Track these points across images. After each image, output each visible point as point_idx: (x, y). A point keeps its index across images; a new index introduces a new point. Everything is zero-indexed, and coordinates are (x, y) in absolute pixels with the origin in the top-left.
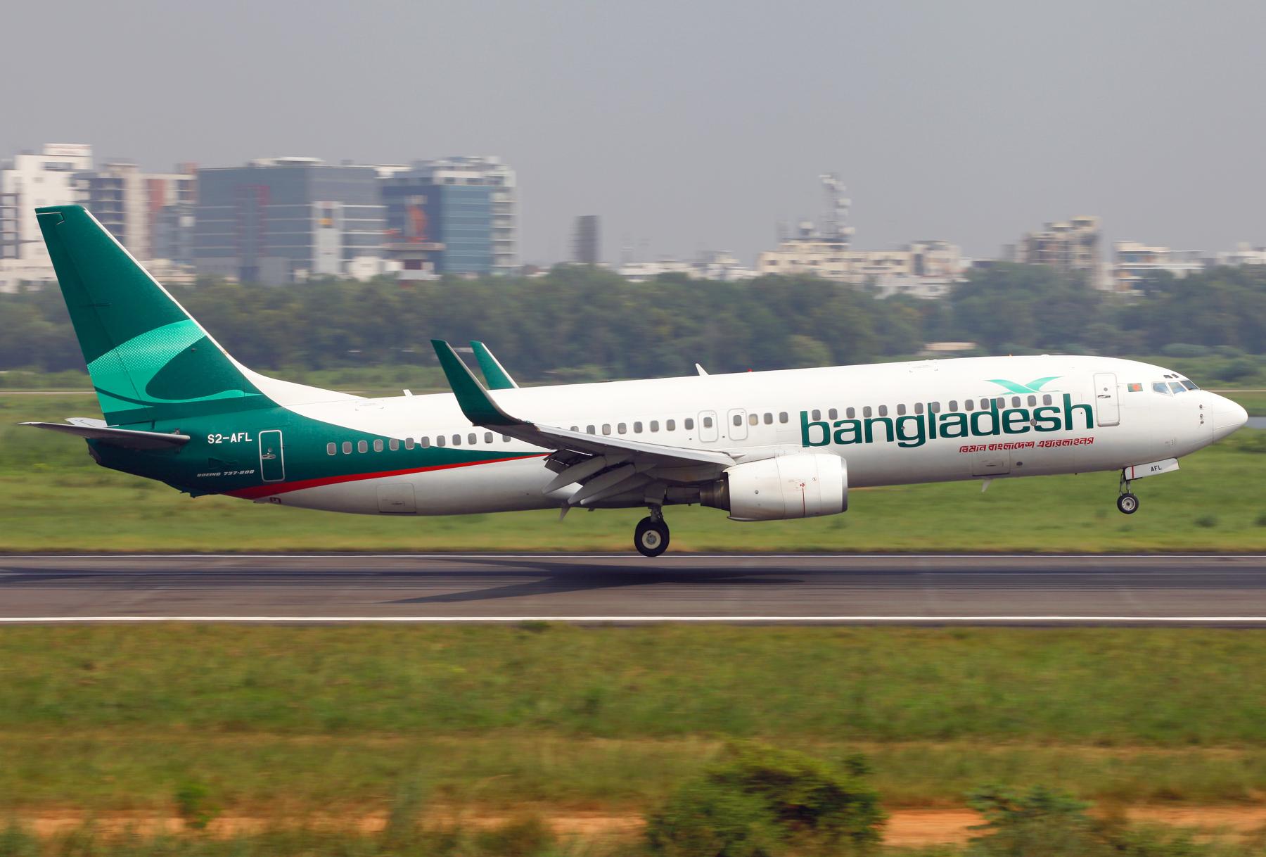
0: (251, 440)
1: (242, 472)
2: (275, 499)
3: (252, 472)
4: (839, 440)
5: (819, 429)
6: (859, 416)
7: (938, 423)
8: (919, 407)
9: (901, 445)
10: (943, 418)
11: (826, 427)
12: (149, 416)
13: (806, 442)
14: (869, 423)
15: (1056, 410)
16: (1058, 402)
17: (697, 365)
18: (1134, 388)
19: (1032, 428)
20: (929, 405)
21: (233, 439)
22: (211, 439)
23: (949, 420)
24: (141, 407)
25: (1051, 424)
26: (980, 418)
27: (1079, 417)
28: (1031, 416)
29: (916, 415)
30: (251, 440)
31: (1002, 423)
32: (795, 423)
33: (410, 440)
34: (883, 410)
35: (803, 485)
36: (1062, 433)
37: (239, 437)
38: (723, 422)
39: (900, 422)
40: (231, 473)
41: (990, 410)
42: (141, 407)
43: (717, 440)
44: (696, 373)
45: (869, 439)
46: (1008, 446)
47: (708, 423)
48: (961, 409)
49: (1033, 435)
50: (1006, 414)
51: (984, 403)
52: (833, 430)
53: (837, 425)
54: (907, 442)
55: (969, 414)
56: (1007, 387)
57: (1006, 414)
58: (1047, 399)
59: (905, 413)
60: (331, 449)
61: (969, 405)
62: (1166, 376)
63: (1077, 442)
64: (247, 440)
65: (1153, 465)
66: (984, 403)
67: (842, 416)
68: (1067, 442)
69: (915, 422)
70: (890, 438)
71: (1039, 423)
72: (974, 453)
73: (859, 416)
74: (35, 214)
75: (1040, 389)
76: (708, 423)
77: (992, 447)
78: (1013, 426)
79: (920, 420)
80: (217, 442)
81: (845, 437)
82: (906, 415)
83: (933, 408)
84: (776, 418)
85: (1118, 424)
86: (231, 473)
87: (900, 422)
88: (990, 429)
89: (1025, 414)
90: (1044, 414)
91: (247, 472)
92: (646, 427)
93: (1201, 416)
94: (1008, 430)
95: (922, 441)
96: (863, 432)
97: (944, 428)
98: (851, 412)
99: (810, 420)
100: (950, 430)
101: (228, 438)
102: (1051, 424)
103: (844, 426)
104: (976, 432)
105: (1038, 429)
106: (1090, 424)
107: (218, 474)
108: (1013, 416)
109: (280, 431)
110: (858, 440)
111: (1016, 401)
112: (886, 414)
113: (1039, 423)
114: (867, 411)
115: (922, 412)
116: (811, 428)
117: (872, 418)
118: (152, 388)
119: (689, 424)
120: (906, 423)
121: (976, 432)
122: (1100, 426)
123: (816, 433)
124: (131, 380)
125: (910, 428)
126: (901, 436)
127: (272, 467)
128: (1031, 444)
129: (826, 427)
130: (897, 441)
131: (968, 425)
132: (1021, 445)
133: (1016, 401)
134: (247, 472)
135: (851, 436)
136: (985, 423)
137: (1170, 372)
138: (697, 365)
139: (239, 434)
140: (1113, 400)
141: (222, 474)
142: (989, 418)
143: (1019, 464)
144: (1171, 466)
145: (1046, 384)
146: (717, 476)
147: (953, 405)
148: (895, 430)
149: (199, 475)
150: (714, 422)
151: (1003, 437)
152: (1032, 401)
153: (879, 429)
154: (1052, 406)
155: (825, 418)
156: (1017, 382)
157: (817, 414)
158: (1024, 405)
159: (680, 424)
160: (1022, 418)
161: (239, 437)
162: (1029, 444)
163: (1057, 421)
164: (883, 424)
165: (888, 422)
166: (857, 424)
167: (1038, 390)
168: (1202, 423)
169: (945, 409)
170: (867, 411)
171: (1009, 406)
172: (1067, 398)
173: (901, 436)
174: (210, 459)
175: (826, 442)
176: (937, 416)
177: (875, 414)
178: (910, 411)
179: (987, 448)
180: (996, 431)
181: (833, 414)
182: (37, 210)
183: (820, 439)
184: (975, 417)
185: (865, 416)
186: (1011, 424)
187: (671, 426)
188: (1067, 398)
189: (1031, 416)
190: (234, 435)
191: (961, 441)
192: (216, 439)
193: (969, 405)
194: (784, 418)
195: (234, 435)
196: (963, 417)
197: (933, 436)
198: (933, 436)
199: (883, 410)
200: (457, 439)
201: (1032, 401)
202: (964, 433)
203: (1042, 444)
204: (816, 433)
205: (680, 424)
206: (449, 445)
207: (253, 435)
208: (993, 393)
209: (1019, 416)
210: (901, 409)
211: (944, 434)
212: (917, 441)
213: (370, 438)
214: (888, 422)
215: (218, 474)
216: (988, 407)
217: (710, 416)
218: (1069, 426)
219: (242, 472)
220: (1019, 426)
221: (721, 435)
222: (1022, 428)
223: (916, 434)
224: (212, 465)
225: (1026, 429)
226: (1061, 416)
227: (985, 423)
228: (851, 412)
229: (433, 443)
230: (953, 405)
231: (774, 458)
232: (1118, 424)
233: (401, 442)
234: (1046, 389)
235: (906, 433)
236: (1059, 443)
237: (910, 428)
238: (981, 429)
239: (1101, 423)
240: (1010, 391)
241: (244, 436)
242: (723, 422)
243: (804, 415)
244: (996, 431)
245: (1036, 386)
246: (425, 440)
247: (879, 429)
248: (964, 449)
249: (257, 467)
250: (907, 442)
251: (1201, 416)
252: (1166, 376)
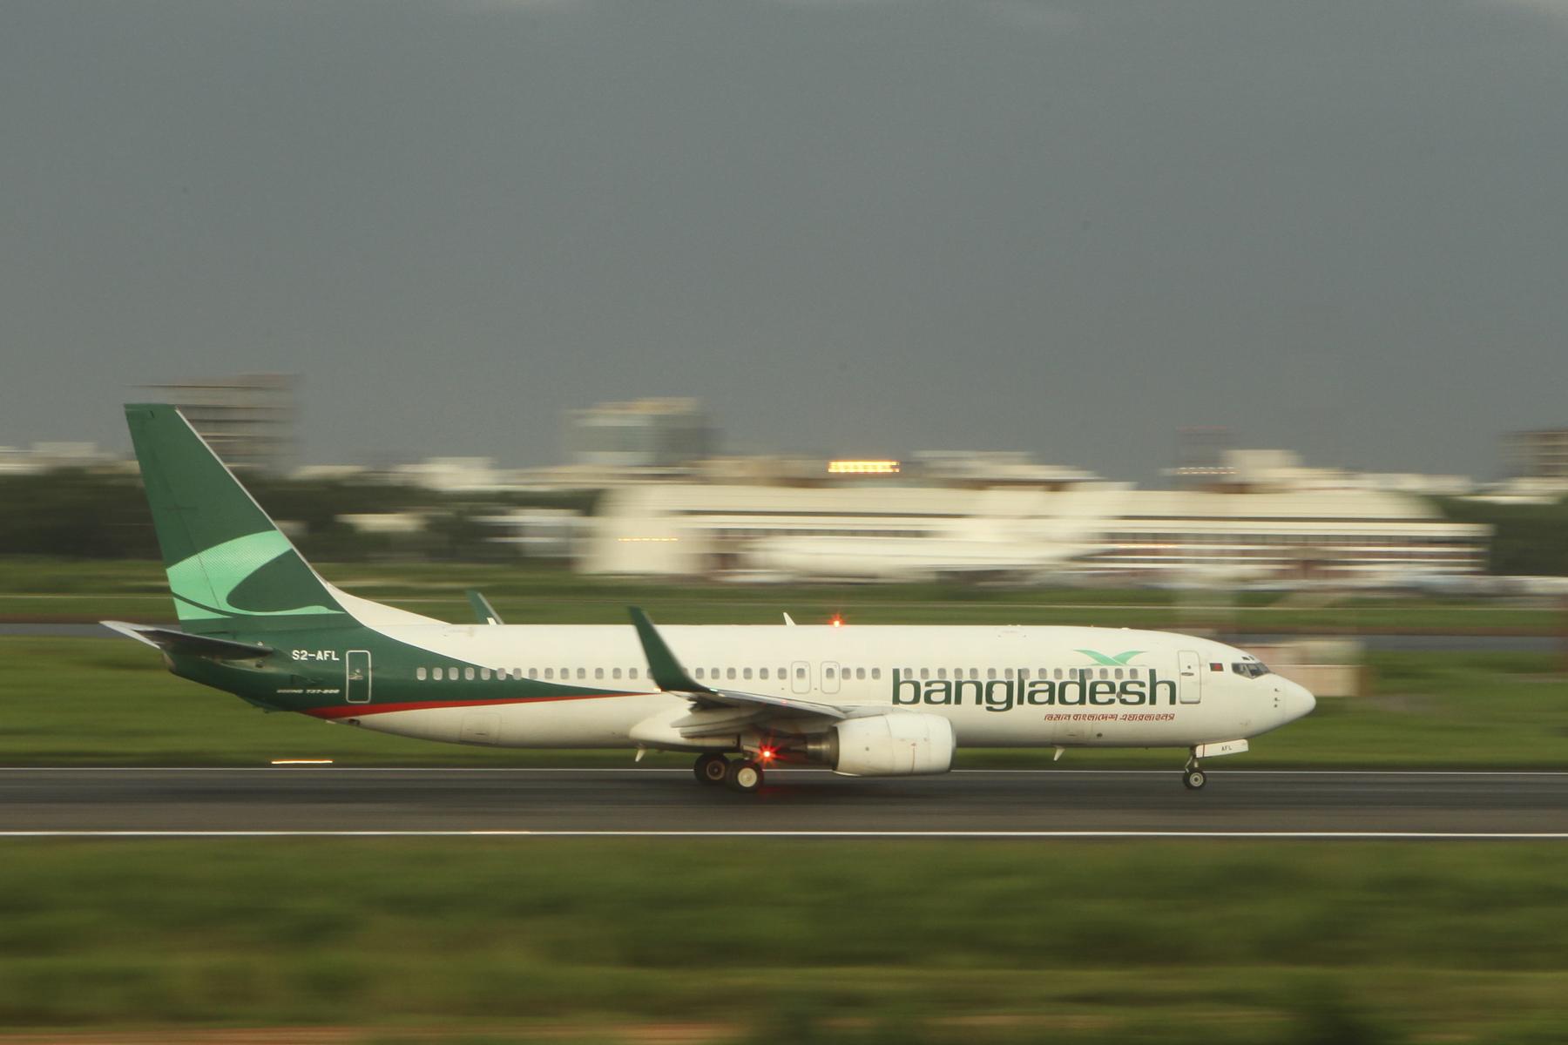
0: (338, 659)
1: (326, 691)
2: (352, 721)
3: (337, 691)
4: (928, 700)
5: (911, 688)
6: (952, 678)
7: (1027, 690)
8: (1009, 672)
9: (989, 709)
10: (1032, 684)
11: (917, 686)
12: (228, 625)
13: (896, 700)
14: (959, 685)
15: (1142, 684)
16: (1145, 678)
17: (786, 615)
18: (1216, 667)
19: (1117, 701)
20: (1020, 671)
21: (319, 656)
22: (296, 655)
23: (1038, 687)
24: (220, 616)
25: (1136, 698)
26: (1068, 687)
27: (1163, 692)
28: (1118, 689)
29: (1006, 681)
30: (338, 659)
31: (1088, 694)
32: (887, 680)
33: (502, 670)
34: (974, 671)
35: (914, 745)
36: (1146, 708)
37: (326, 655)
38: (816, 674)
39: (990, 686)
40: (314, 691)
41: (1078, 680)
42: (220, 616)
43: (808, 693)
44: (783, 622)
45: (958, 701)
46: (1092, 717)
47: (801, 672)
48: (1050, 677)
49: (1117, 708)
50: (1094, 685)
51: (1072, 671)
52: (924, 689)
53: (928, 684)
54: (995, 707)
56: (1097, 659)
57: (1094, 685)
58: (1134, 672)
59: (994, 678)
60: (421, 675)
61: (1058, 672)
62: (1245, 658)
63: (1159, 717)
64: (334, 659)
65: (1224, 744)
66: (1072, 671)
67: (934, 676)
68: (1149, 717)
69: (1005, 687)
70: (979, 701)
71: (1124, 696)
72: (1058, 722)
73: (952, 678)
74: (123, 410)
75: (1128, 662)
76: (801, 672)
77: (1076, 717)
78: (1099, 698)
79: (1010, 685)
80: (302, 658)
81: (934, 697)
82: (997, 679)
84: (868, 673)
85: (1198, 702)
86: (314, 691)
87: (990, 686)
88: (1077, 699)
89: (1112, 686)
90: (1130, 688)
91: (331, 691)
92: (740, 673)
93: (1276, 699)
94: (1093, 701)
95: (1009, 706)
96: (953, 694)
97: (1032, 695)
98: (942, 672)
99: (902, 678)
100: (1038, 697)
101: (310, 655)
102: (1136, 698)
103: (934, 686)
104: (1063, 701)
105: (1123, 702)
106: (1173, 701)
107: (300, 691)
108: (1100, 688)
109: (369, 653)
110: (947, 701)
111: (1104, 672)
112: (945, 677)
113: (1124, 696)
114: (958, 672)
115: (1012, 677)
116: (902, 687)
117: (963, 680)
118: (233, 598)
119: (782, 673)
120: (996, 688)
121: (1063, 701)
122: (1182, 703)
123: (907, 692)
124: (212, 588)
125: (1000, 693)
126: (990, 700)
127: (359, 688)
128: (1114, 717)
129: (917, 686)
130: (985, 704)
131: (1056, 693)
132: (1105, 717)
133: (1104, 672)
134: (331, 691)
135: (941, 696)
136: (1072, 693)
137: (1246, 655)
138: (786, 615)
139: (326, 652)
140: (1195, 678)
141: (305, 691)
142: (1077, 688)
143: (1099, 735)
144: (1240, 746)
145: (1132, 659)
146: (825, 730)
147: (1042, 672)
148: (984, 694)
149: (279, 691)
150: (807, 673)
151: (1089, 708)
152: (1119, 673)
153: (969, 692)
154: (1139, 680)
155: (916, 677)
156: (1105, 655)
157: (908, 671)
158: (1111, 678)
159: (773, 673)
160: (1108, 690)
161: (326, 655)
162: (1112, 717)
163: (1142, 696)
164: (973, 687)
165: (979, 685)
166: (948, 685)
167: (1125, 663)
168: (1276, 706)
169: (1034, 677)
170: (958, 672)
171: (1096, 677)
172: (1152, 673)
173: (990, 700)
174: (292, 676)
175: (916, 700)
177: (966, 677)
178: (1001, 676)
179: (1072, 717)
180: (1082, 701)
181: (925, 672)
182: (127, 406)
183: (911, 697)
184: (1063, 686)
185: (956, 677)
186: (1097, 696)
187: (764, 673)
188: (1152, 673)
189: (1118, 689)
190: (320, 653)
191: (1048, 709)
192: (301, 655)
193: (1058, 672)
194: (876, 673)
195: (320, 653)
196: (1052, 685)
197: (1020, 701)
198: (1020, 701)
199: (974, 671)
200: (549, 672)
201: (1119, 673)
202: (1051, 701)
203: (1125, 717)
204: (907, 692)
205: (773, 673)
206: (541, 678)
207: (340, 654)
208: (1083, 663)
209: (1106, 688)
210: (992, 672)
211: (1032, 700)
212: (1004, 706)
213: (462, 666)
214: (979, 685)
215: (300, 691)
216: (1074, 678)
217: (803, 667)
218: (1153, 701)
219: (326, 691)
221: (813, 689)
222: (1106, 700)
223: (1004, 698)
224: (293, 681)
225: (1111, 701)
226: (1146, 691)
227: (1072, 693)
228: (942, 672)
229: (525, 675)
230: (1042, 672)
231: (882, 715)
232: (1198, 702)
233: (493, 673)
234: (1132, 663)
235: (995, 698)
236: (1142, 717)
237: (1000, 693)
238: (1068, 699)
239: (1184, 700)
240: (1096, 662)
241: (330, 654)
242: (816, 674)
243: (896, 672)
244: (1082, 701)
245: (1123, 659)
246: (517, 671)
247: (969, 692)
248: (1050, 717)
249: (342, 689)
250: (995, 707)
251: (1276, 699)
252: (1245, 658)
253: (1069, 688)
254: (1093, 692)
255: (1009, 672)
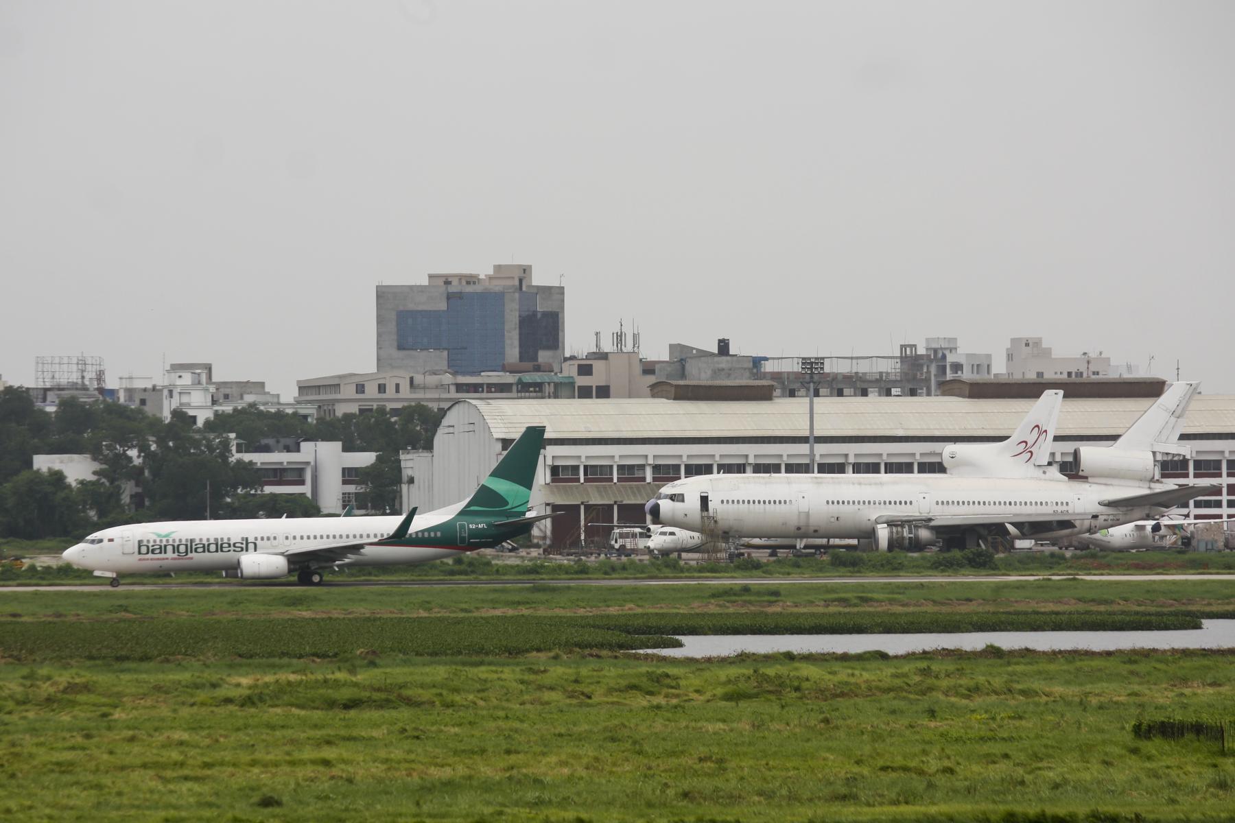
7: (194, 547)
11: (148, 547)
14: (165, 546)
25: (240, 549)
27: (251, 546)
45: (165, 552)
50: (222, 544)
52: (151, 548)
55: (206, 544)
61: (208, 540)
70: (174, 552)
78: (224, 549)
79: (186, 545)
83: (192, 541)
87: (178, 546)
94: (222, 551)
95: (187, 554)
100: (199, 550)
102: (240, 549)
104: (209, 551)
105: (234, 551)
108: (224, 545)
110: (160, 553)
121: (209, 551)
123: (144, 550)
125: (182, 549)
126: (178, 552)
130: (177, 554)
131: (206, 548)
136: (213, 548)
148: (176, 549)
153: (170, 549)
165: (173, 546)
169: (197, 542)
173: (178, 552)
175: (148, 553)
176: (194, 544)
180: (217, 551)
184: (209, 545)
196: (204, 545)
197: (191, 552)
204: (144, 550)
209: (226, 545)
211: (196, 551)
214: (173, 546)
220: (227, 549)
225: (229, 551)
226: (244, 546)
227: (213, 548)
237: (182, 549)
244: (217, 551)
247: (170, 549)
253: (211, 546)
254: (222, 547)
255: (187, 540)
